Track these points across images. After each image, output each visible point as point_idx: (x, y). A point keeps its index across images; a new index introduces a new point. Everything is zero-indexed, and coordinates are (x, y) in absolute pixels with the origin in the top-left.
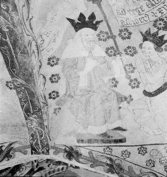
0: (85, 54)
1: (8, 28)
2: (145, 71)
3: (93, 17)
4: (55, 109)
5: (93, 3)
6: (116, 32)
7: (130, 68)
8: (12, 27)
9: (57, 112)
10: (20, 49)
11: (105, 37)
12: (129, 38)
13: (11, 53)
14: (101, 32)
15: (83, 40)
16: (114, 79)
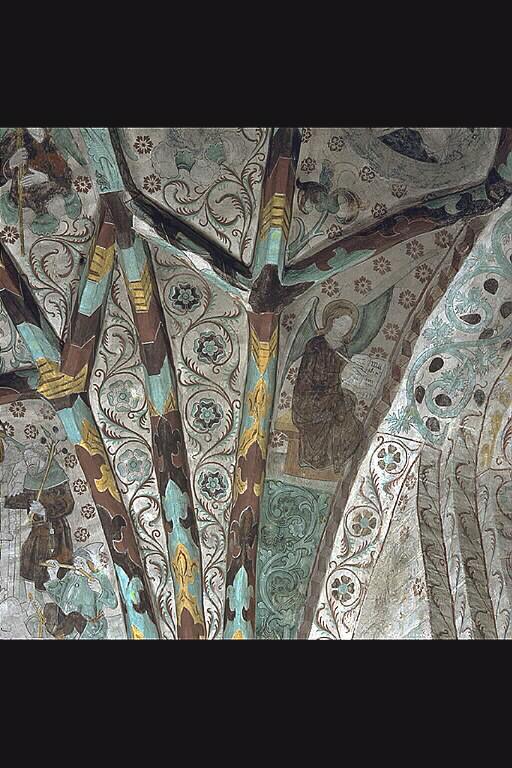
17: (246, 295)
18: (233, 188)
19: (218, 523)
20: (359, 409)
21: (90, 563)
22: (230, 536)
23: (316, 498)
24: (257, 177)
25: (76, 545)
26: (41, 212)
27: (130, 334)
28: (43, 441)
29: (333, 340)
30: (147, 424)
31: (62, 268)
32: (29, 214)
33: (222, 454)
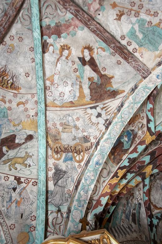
0: (131, 26)
1: (95, 28)
2: (153, 6)
3: (120, 11)
4: (141, 56)
5: (116, 7)
6: (130, 7)
7: (148, 12)
8: (96, 27)
9: (142, 57)
10: (103, 32)
11: (130, 12)
12: (135, 4)
13: (103, 37)
14: (127, 13)
15: (125, 21)
16: (149, 22)
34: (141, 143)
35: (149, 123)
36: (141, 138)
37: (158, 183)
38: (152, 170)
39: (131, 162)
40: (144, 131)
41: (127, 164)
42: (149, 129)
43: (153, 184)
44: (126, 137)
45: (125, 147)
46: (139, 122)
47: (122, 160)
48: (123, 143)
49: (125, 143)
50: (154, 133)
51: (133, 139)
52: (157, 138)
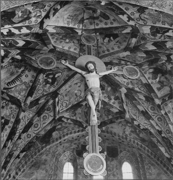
17: (58, 117)
18: (68, 103)
19: (25, 142)
20: (51, 138)
21: (4, 135)
22: (26, 145)
23: (37, 146)
24: (71, 104)
25: (4, 131)
26: (46, 84)
27: (38, 107)
28: (11, 111)
29: (57, 128)
30: (28, 121)
31: (40, 93)
32: (44, 83)
33: (34, 133)
34: (28, 27)
35: (46, 19)
36: (31, 24)
37: (11, 68)
38: (17, 55)
39: (9, 34)
40: (37, 21)
41: (5, 34)
42: (42, 23)
43: (8, 66)
44: (21, 12)
45: (14, 20)
46: (40, 11)
47: (4, 27)
48: (15, 15)
49: (17, 16)
50: (44, 29)
51: (24, 19)
52: (42, 34)
